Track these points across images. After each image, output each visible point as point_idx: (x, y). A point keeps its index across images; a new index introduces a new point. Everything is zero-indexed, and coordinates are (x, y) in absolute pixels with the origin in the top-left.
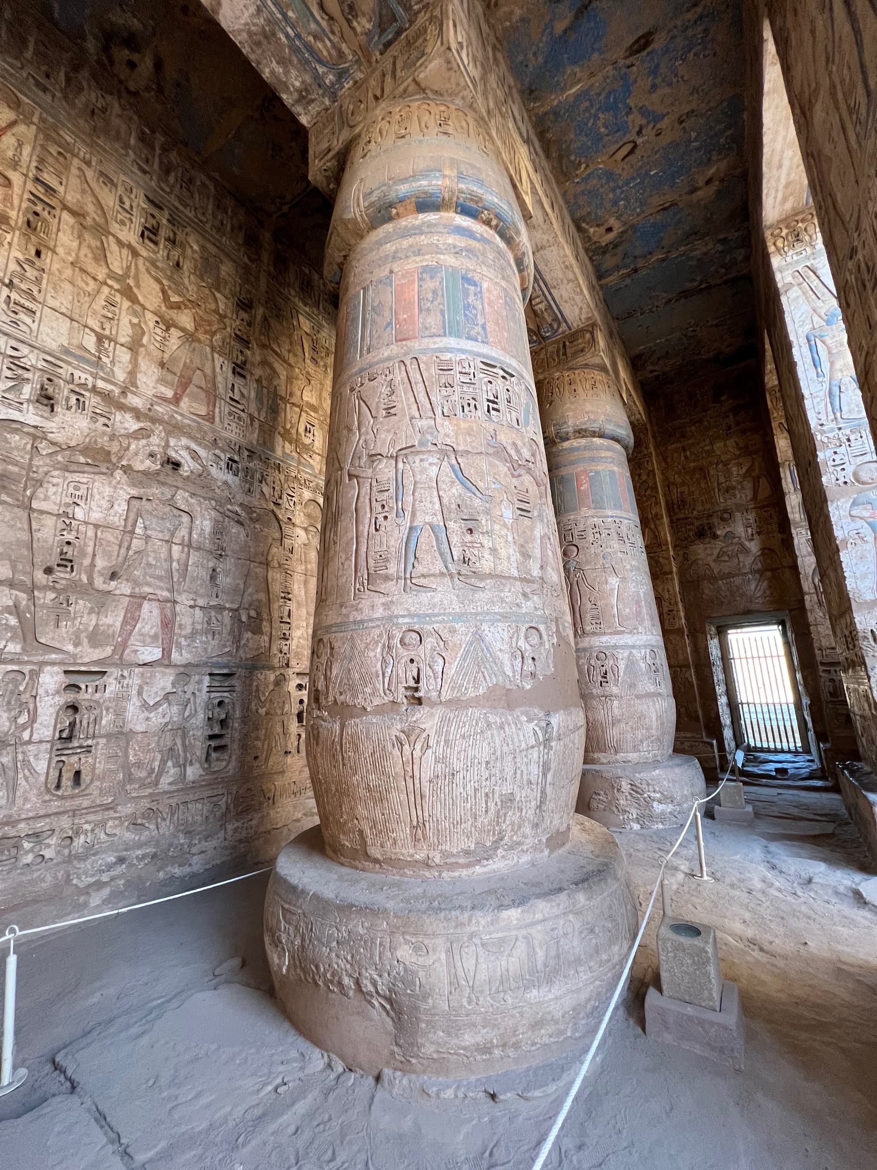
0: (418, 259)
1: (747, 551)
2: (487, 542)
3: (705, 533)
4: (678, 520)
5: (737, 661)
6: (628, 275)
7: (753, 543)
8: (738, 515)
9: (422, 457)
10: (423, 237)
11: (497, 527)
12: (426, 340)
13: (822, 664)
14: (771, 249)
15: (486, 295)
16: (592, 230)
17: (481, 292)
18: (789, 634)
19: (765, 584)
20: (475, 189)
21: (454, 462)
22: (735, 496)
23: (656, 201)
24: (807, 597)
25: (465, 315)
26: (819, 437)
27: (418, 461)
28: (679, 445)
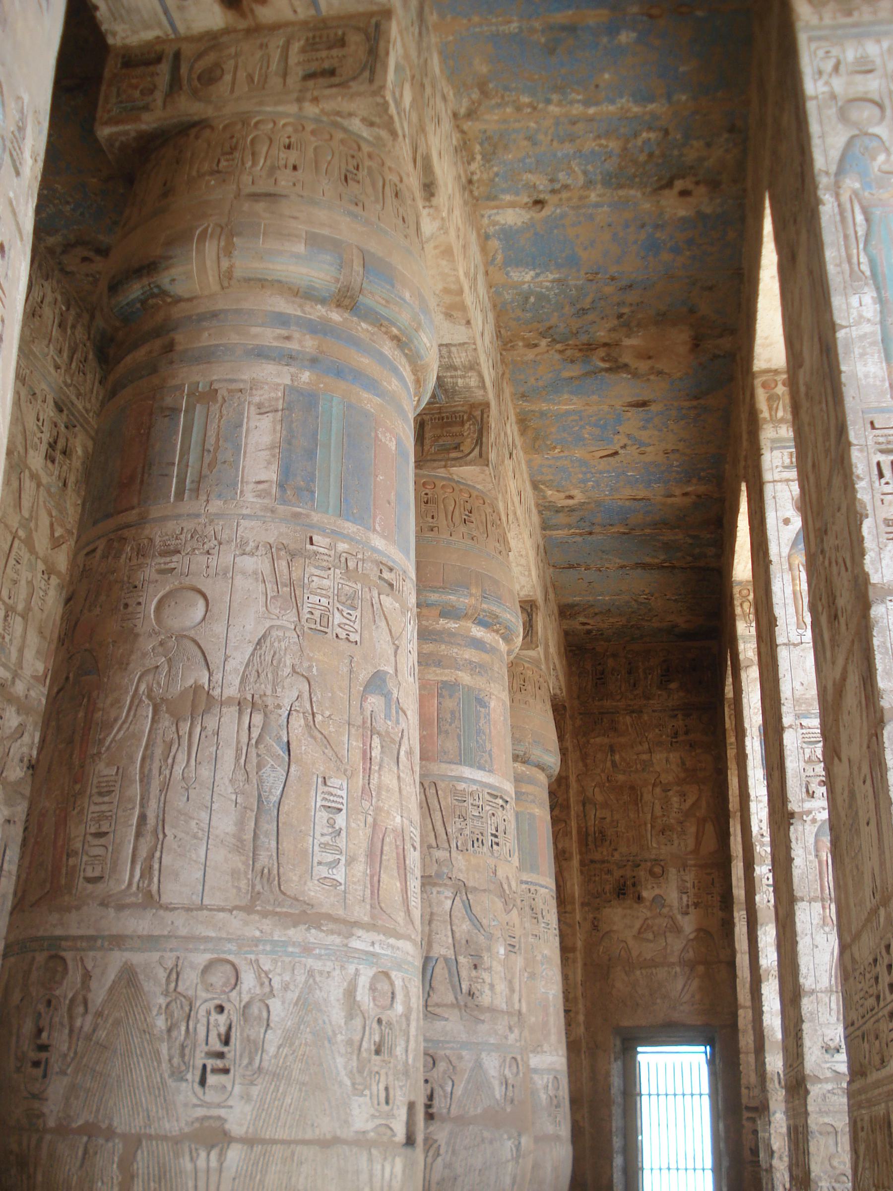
0: (439, 671)
1: (677, 930)
2: (485, 975)
3: (626, 890)
4: (592, 861)
5: (645, 1099)
6: (581, 535)
7: (687, 918)
8: (673, 871)
9: (439, 889)
10: (443, 647)
11: (495, 964)
12: (444, 766)
13: (748, 1109)
14: (738, 610)
15: (492, 716)
16: (550, 493)
17: (489, 714)
18: (717, 1061)
19: (695, 984)
20: (494, 609)
21: (464, 897)
22: (671, 841)
23: (628, 492)
24: (741, 1012)
25: (477, 741)
26: (758, 848)
27: (435, 893)
28: (606, 740)
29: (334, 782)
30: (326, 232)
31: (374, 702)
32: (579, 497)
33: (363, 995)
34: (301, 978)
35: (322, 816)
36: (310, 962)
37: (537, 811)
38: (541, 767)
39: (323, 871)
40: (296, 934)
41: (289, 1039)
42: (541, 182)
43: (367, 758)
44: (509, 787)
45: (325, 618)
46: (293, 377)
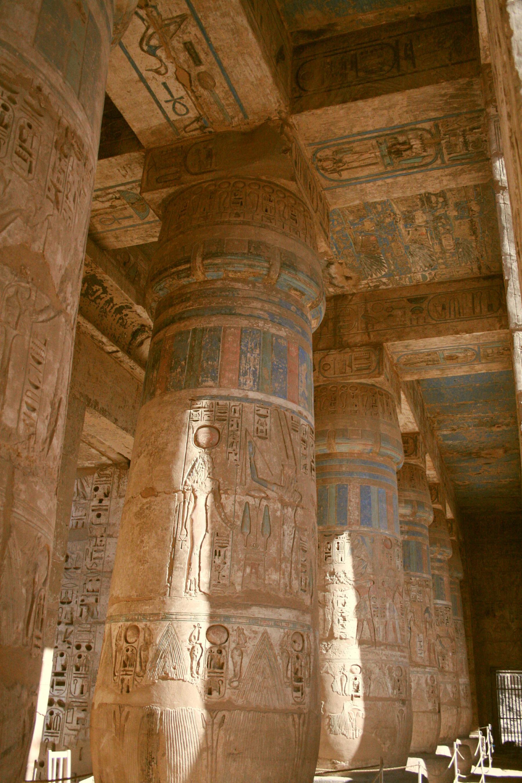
29: (420, 635)
30: (408, 498)
31: (427, 614)
32: (467, 482)
33: (429, 681)
34: (417, 678)
35: (418, 643)
36: (419, 675)
37: (456, 594)
38: (457, 578)
39: (419, 655)
40: (415, 669)
41: (416, 691)
42: (455, 427)
43: (426, 628)
44: (450, 604)
45: (416, 598)
46: (404, 538)
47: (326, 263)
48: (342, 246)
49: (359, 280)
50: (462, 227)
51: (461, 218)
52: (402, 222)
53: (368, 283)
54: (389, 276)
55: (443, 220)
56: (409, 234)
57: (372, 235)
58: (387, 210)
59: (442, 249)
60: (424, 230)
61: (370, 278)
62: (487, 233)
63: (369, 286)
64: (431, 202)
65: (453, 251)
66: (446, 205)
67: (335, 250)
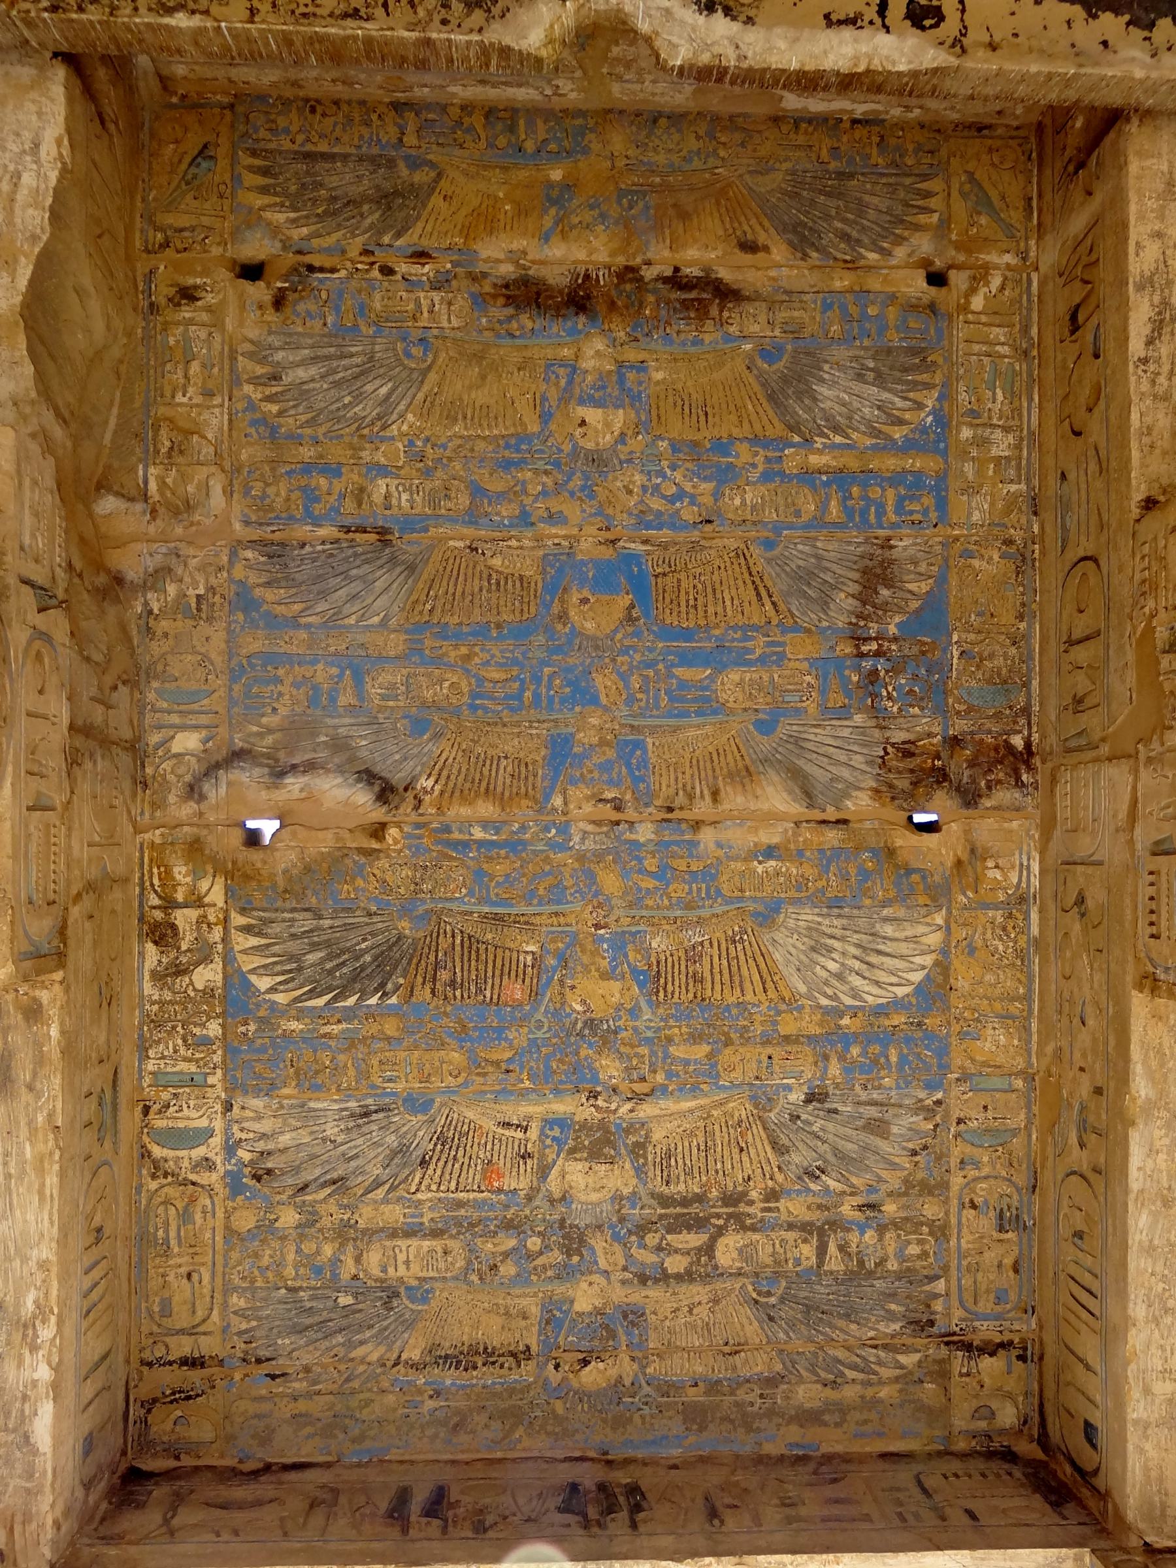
47: (398, 778)
48: (499, 869)
49: (237, 878)
50: (496, 1322)
51: (549, 1321)
52: (586, 1112)
53: (198, 902)
54: (234, 997)
55: (557, 1256)
56: (507, 1125)
57: (535, 995)
58: (670, 1075)
59: (370, 1234)
60: (519, 1181)
61: (238, 920)
62: (431, 1404)
63: (169, 904)
64: (669, 1231)
65: (349, 1268)
66: (643, 1279)
67: (478, 833)
